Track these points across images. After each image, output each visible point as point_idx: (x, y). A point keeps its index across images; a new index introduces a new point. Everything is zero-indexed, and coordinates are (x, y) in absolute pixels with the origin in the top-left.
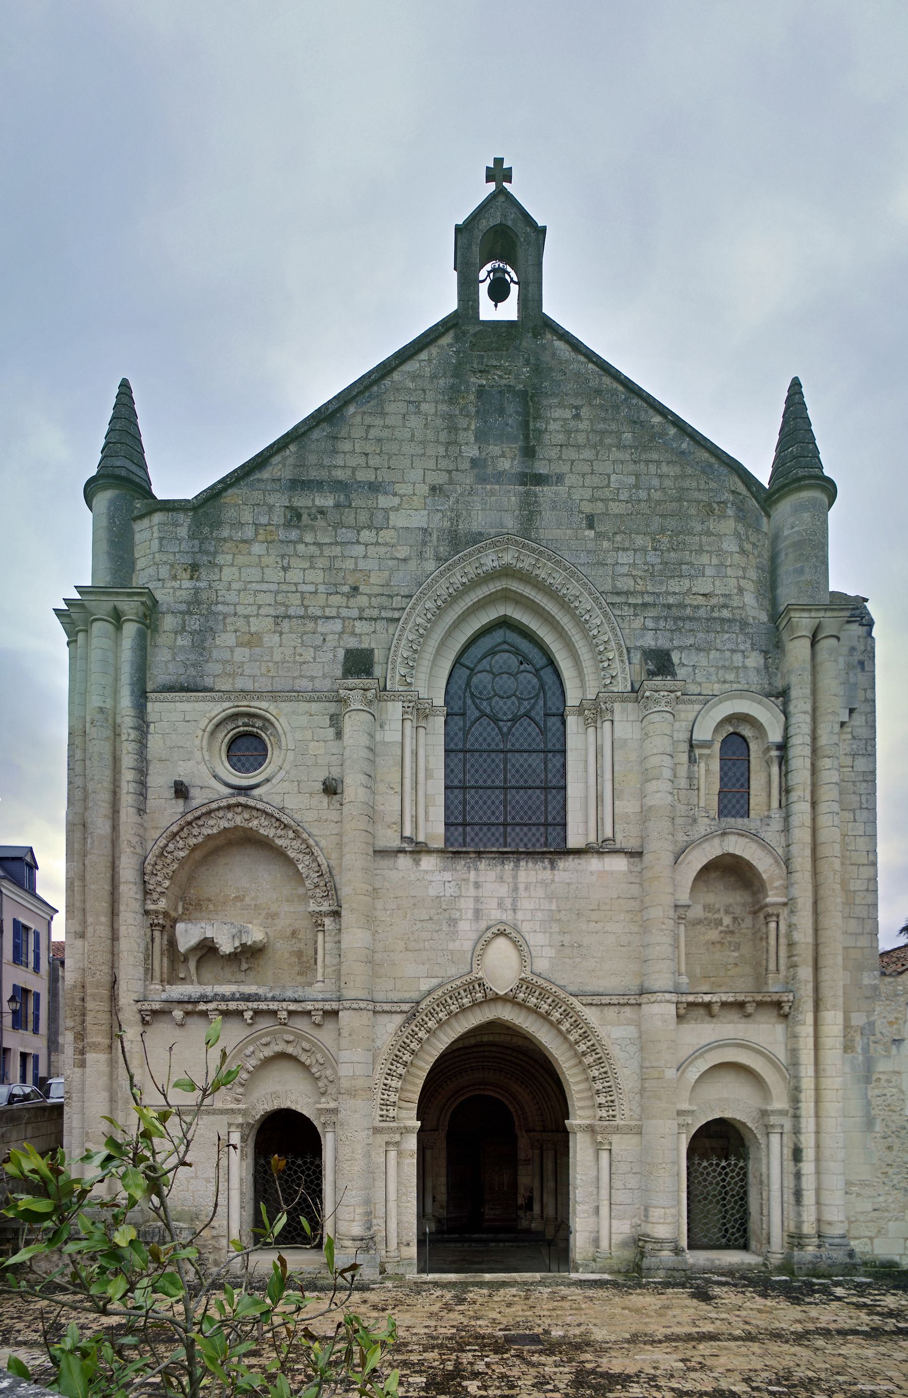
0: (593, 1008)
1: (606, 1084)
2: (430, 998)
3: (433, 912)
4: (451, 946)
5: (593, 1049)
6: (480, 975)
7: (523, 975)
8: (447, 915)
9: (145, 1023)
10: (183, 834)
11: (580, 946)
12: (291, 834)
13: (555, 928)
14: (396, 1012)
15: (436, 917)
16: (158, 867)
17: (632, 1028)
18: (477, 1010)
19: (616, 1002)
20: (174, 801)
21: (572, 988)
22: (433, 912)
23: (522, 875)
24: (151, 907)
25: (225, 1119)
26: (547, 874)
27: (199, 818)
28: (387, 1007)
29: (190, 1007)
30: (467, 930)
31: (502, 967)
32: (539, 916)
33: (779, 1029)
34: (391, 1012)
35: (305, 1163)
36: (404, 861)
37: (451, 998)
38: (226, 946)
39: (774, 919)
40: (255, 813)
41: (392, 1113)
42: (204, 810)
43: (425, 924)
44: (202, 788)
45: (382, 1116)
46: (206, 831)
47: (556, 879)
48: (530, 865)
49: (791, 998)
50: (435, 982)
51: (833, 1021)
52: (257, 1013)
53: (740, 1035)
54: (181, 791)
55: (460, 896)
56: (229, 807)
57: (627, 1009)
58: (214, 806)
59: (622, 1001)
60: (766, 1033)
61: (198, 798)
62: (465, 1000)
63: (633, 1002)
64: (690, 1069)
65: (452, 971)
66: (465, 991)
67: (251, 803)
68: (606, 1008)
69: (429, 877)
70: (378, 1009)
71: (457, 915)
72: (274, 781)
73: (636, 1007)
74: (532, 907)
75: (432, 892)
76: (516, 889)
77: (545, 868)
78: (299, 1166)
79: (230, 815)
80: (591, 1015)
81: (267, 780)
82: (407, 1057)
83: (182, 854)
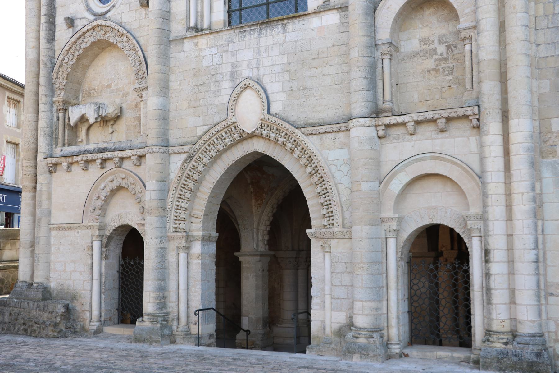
0: (315, 137)
1: (327, 198)
2: (201, 141)
3: (205, 78)
4: (217, 101)
5: (316, 171)
6: (233, 120)
7: (263, 117)
8: (214, 79)
9: (51, 172)
10: (72, 51)
11: (304, 89)
12: (125, 39)
13: (287, 77)
14: (181, 153)
15: (207, 82)
16: (60, 74)
17: (345, 151)
18: (239, 146)
19: (330, 130)
20: (68, 31)
21: (300, 123)
22: (205, 78)
23: (263, 39)
24: (54, 99)
25: (89, 232)
26: (280, 38)
27: (79, 38)
28: (176, 149)
29: (70, 160)
30: (226, 87)
31: (249, 113)
32: (276, 69)
33: (473, 141)
34: (178, 153)
35: (135, 263)
36: (188, 45)
37: (217, 139)
38: (92, 120)
39: (468, 41)
40: (106, 29)
41: (182, 226)
42: (80, 33)
43: (200, 87)
44: (80, 19)
45: (175, 228)
46: (83, 46)
47: (287, 40)
48: (268, 31)
49: (476, 111)
50: (206, 128)
51: (521, 128)
52: (104, 161)
53: (437, 149)
54: (70, 22)
55: (222, 63)
56: (93, 28)
57: (341, 135)
58: (85, 29)
59: (335, 129)
60: (458, 143)
61: (79, 24)
62: (227, 140)
63: (343, 129)
64: (394, 181)
65: (217, 119)
66: (226, 133)
67: (104, 23)
68: (324, 136)
69: (203, 54)
70: (170, 152)
71: (220, 77)
72: (116, 6)
73: (348, 132)
74: (270, 64)
75: (205, 64)
76: (259, 53)
77: (279, 33)
78: (132, 266)
79: (94, 34)
80: (312, 143)
81: (113, 6)
82: (191, 185)
83: (71, 63)
